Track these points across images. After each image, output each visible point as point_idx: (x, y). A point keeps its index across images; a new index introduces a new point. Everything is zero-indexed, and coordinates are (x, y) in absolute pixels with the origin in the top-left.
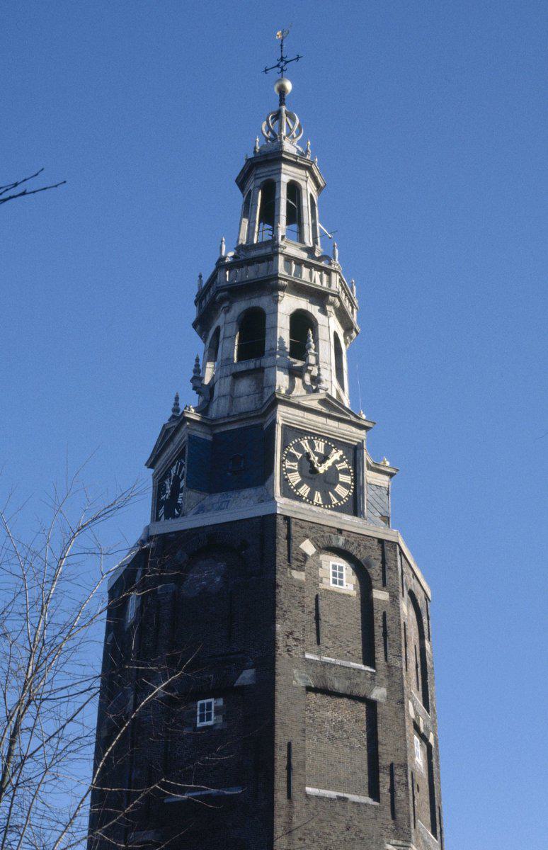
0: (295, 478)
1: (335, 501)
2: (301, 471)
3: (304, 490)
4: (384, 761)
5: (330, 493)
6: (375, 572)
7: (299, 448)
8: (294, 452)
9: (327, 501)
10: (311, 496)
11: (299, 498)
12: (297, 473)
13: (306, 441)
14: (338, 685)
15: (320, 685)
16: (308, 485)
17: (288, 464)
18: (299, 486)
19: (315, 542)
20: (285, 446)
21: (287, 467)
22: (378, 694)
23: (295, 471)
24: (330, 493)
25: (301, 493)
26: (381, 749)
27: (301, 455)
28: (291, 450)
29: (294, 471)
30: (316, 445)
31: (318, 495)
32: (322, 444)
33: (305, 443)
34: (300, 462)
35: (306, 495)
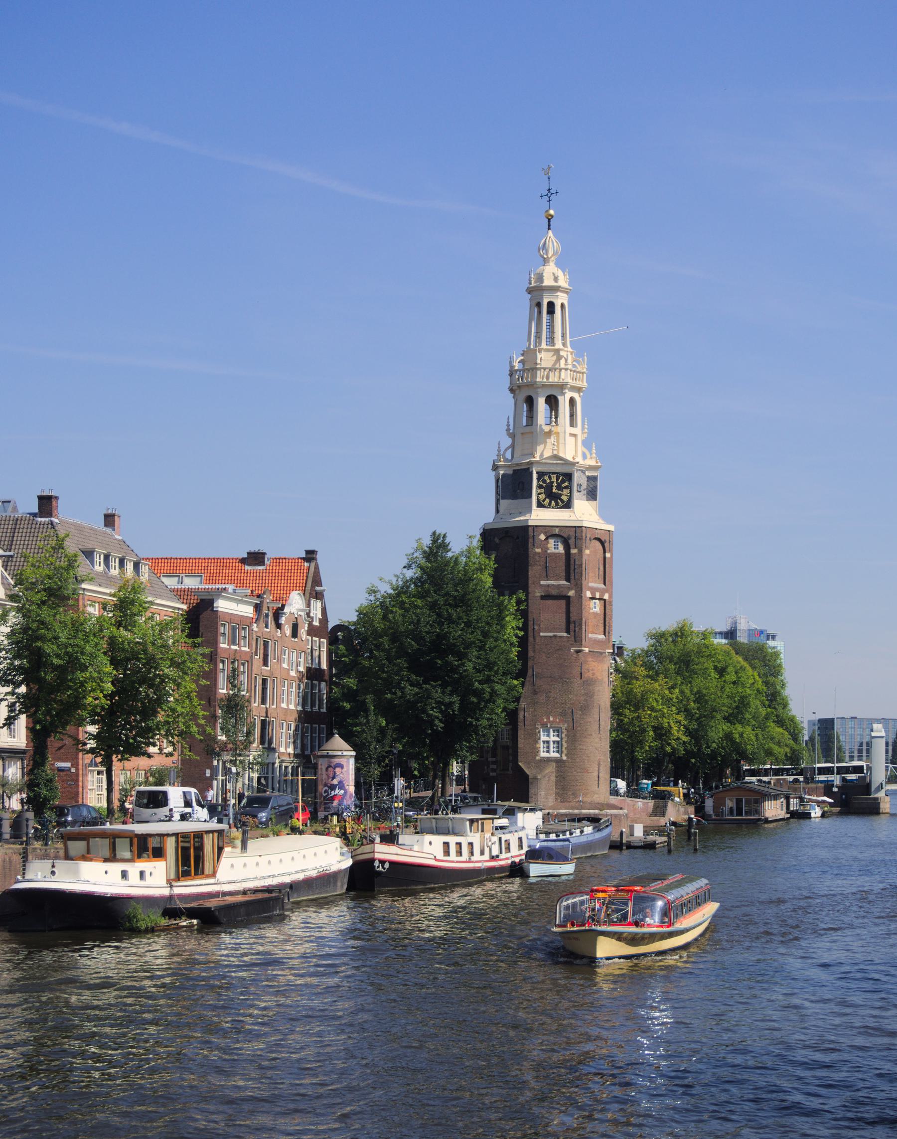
0: (542, 497)
3: (548, 500)
4: (572, 619)
6: (571, 542)
7: (544, 481)
9: (557, 504)
10: (550, 504)
14: (554, 592)
15: (547, 594)
18: (544, 501)
19: (545, 533)
20: (538, 479)
22: (571, 593)
26: (571, 615)
31: (553, 503)
33: (546, 478)
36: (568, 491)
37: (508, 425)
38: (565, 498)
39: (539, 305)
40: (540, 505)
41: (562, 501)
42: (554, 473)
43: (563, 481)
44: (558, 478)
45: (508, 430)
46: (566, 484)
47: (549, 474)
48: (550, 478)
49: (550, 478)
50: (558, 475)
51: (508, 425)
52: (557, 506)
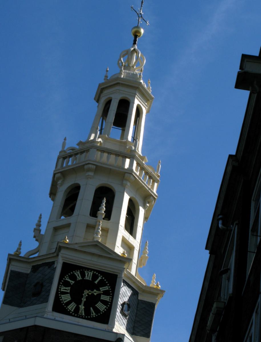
0: (66, 298)
1: (94, 314)
2: (71, 293)
5: (91, 308)
8: (69, 280)
11: (68, 313)
12: (69, 294)
13: (79, 272)
16: (75, 303)
17: (63, 289)
21: (62, 290)
23: (67, 293)
24: (91, 308)
25: (70, 308)
27: (73, 282)
28: (67, 279)
29: (67, 293)
30: (86, 274)
32: (91, 274)
34: (72, 287)
35: (72, 311)
36: (107, 298)
37: (39, 225)
38: (101, 307)
39: (108, 103)
40: (59, 307)
41: (97, 310)
42: (88, 269)
43: (102, 284)
44: (95, 277)
45: (37, 230)
46: (106, 288)
47: (83, 269)
48: (83, 275)
49: (83, 275)
50: (97, 273)
51: (39, 225)
52: (87, 316)
